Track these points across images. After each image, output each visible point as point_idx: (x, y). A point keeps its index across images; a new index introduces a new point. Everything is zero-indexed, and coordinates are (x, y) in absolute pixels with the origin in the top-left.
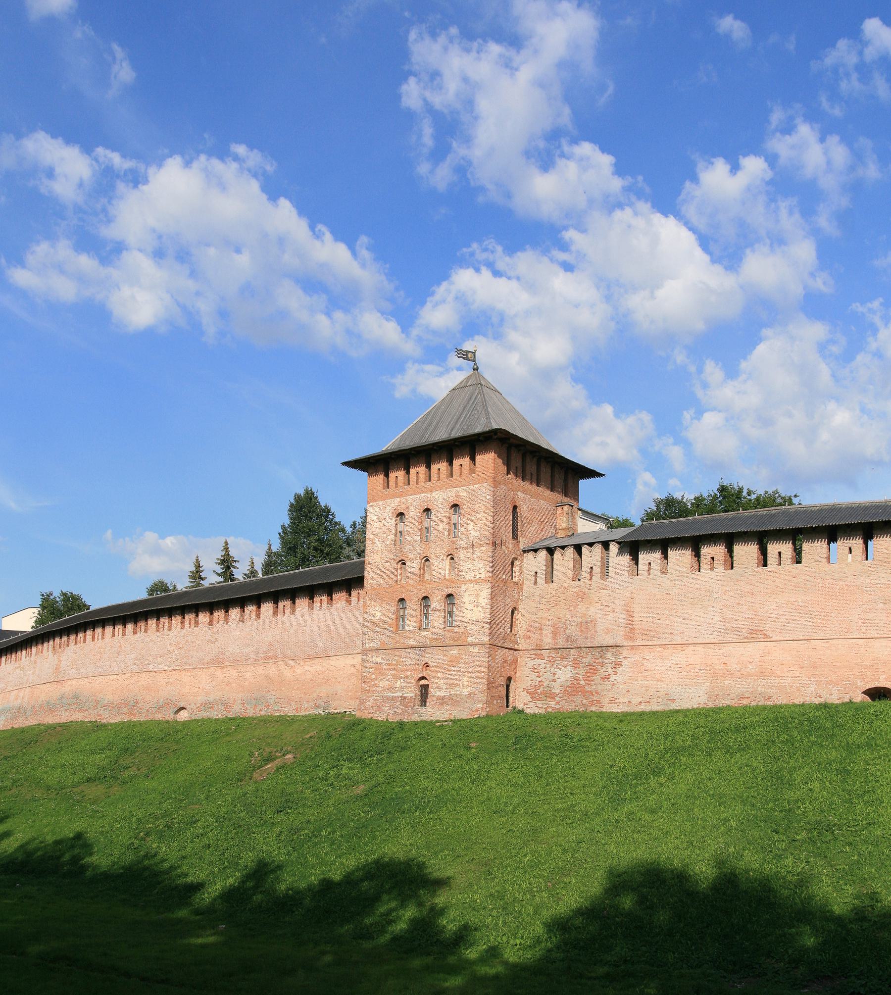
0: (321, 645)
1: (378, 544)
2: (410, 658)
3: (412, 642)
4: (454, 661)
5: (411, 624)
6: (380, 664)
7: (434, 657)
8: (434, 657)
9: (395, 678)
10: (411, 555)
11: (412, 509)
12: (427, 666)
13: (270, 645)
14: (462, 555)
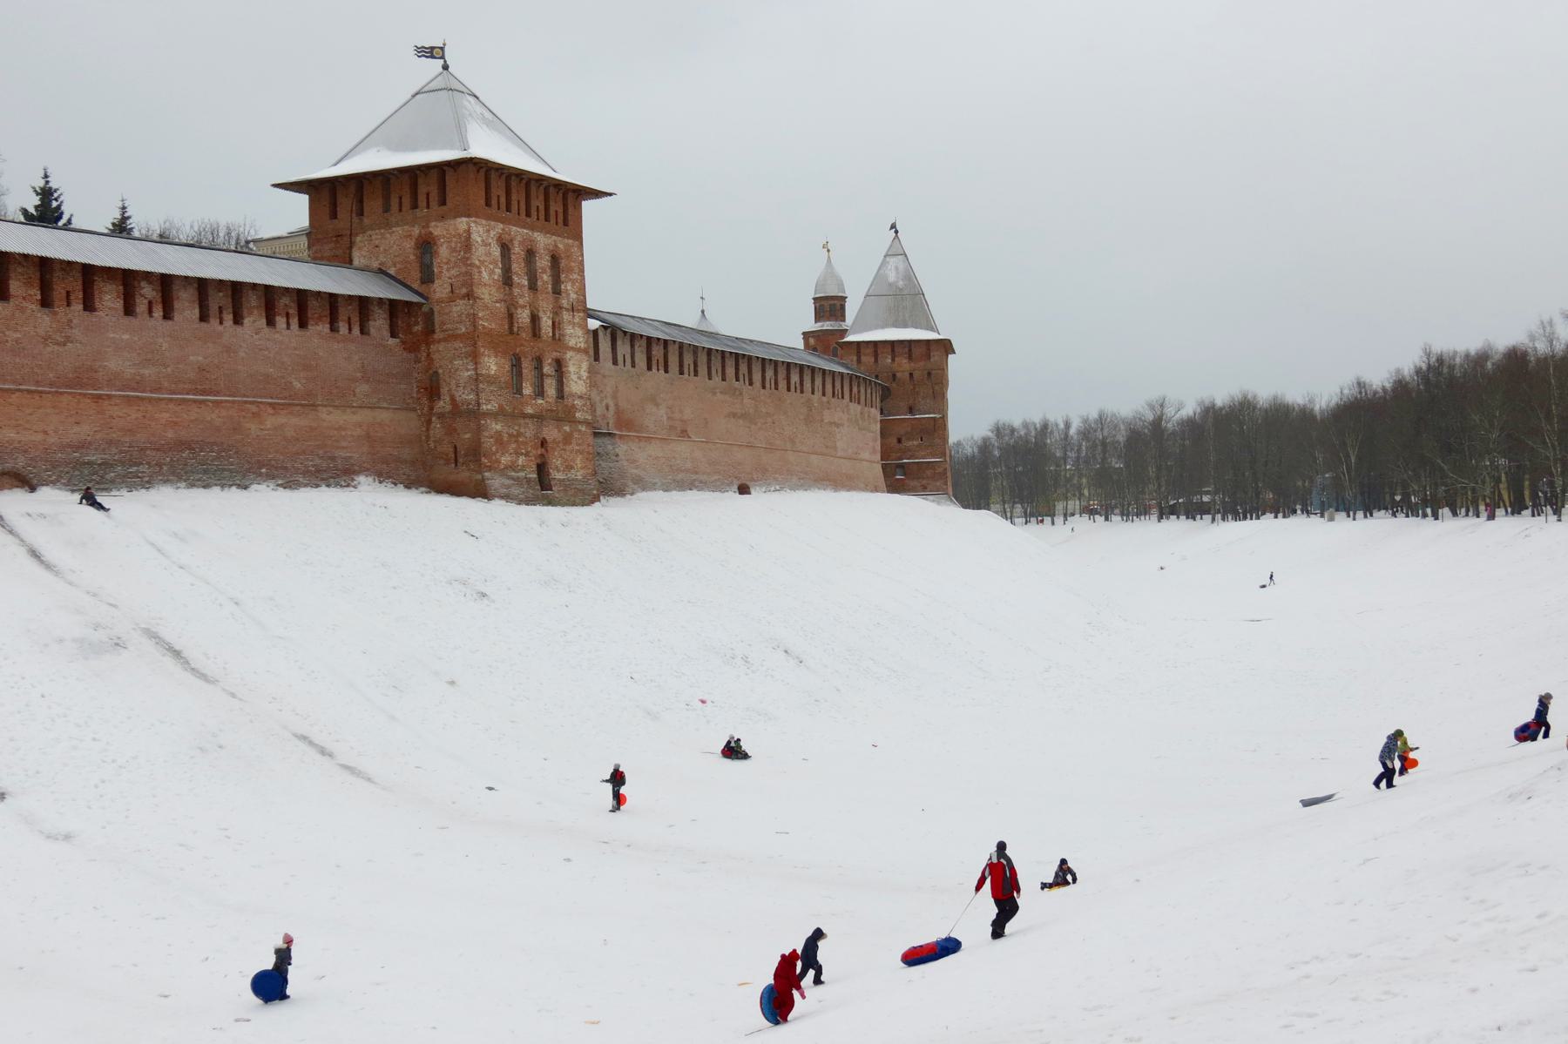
0: (297, 385)
1: (485, 274)
2: (529, 430)
3: (529, 410)
4: (567, 439)
5: (527, 390)
6: (499, 433)
7: (551, 433)
8: (551, 433)
9: (518, 454)
10: (521, 302)
11: (516, 243)
12: (543, 443)
13: (201, 369)
14: (566, 316)
